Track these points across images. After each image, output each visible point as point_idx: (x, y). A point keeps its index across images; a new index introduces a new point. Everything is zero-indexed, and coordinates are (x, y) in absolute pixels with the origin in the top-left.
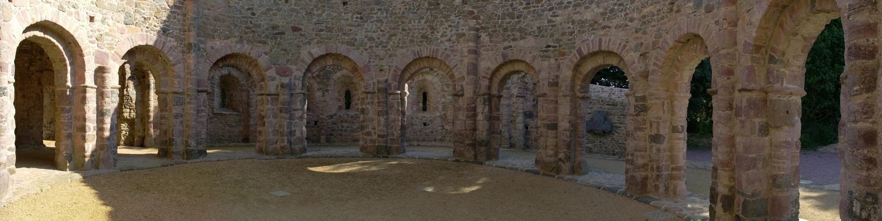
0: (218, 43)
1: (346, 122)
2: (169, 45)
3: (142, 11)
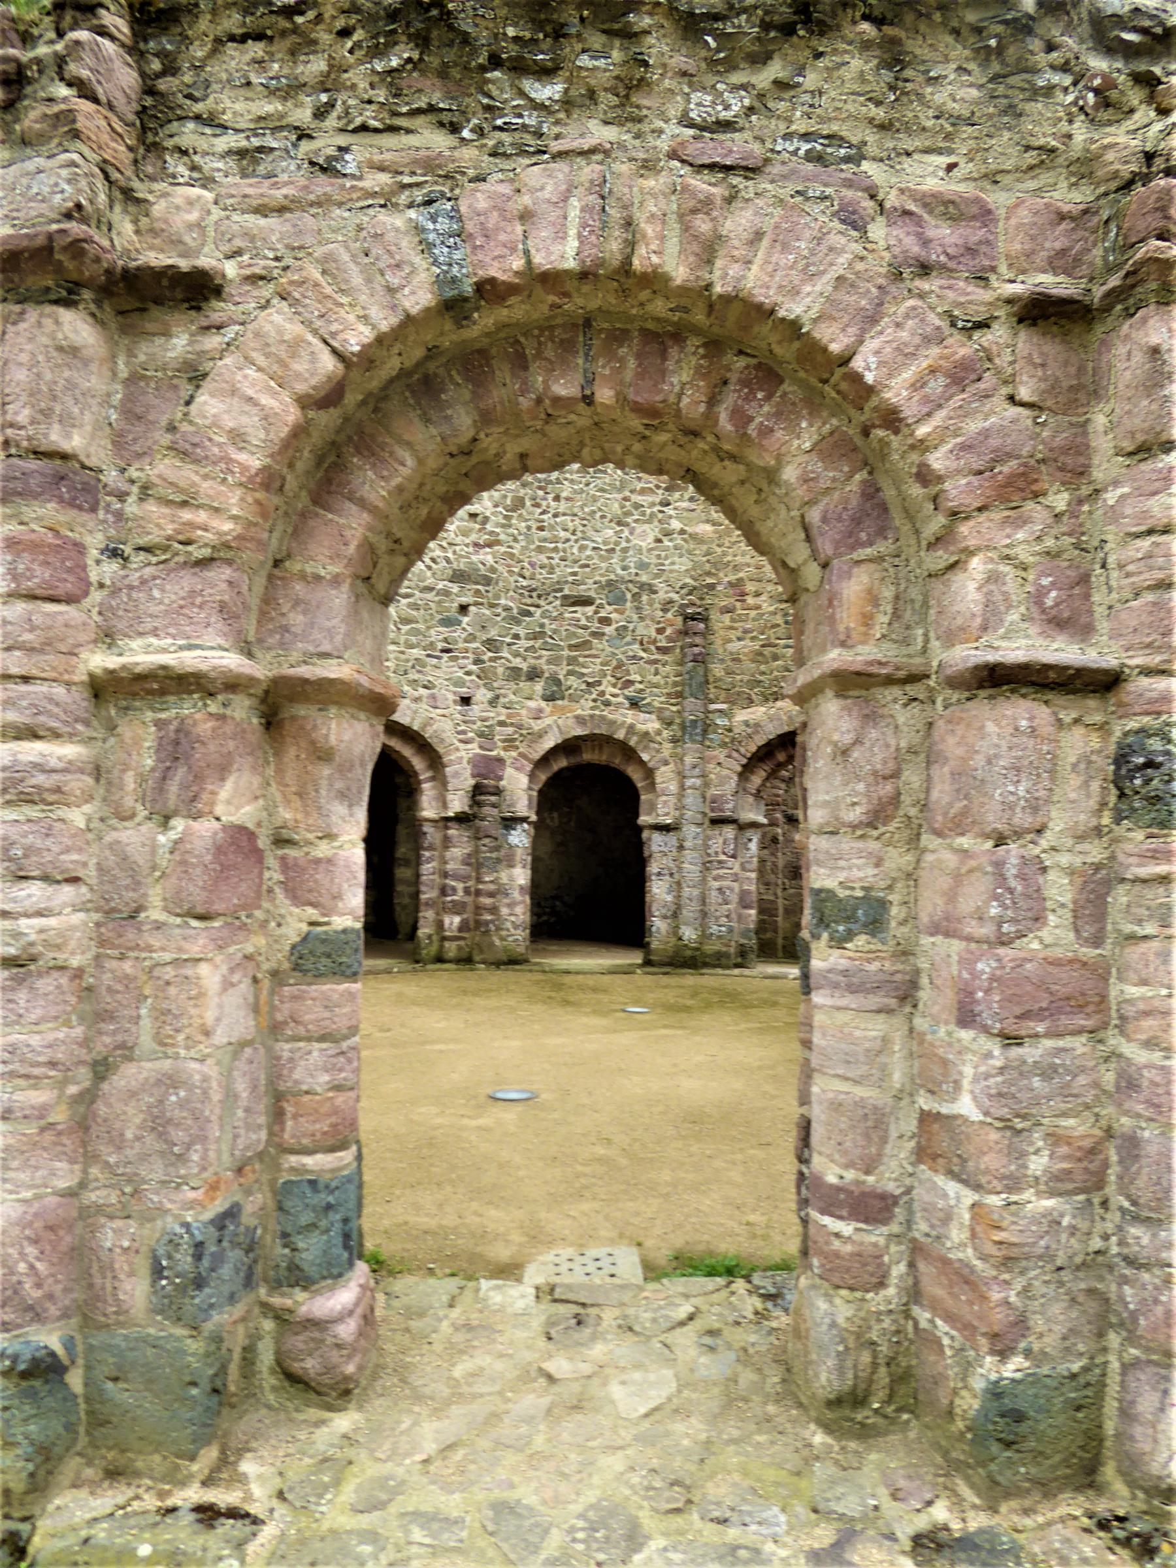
0: (758, 713)
3: (584, 671)
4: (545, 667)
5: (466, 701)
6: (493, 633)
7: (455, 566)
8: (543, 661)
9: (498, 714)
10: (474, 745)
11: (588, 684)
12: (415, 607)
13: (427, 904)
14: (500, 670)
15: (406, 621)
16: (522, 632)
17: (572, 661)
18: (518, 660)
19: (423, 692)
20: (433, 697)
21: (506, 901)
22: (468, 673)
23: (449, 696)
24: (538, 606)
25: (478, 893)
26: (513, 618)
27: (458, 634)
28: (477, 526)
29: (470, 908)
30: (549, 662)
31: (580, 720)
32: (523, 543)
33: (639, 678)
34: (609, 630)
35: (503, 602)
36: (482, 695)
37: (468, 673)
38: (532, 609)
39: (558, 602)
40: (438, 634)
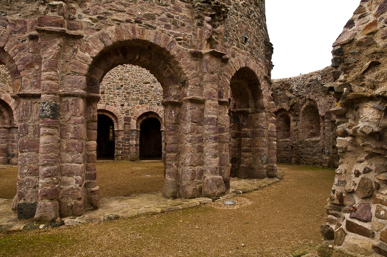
1: (309, 146)
2: (160, 110)
3: (148, 98)
4: (140, 97)
5: (122, 105)
6: (129, 91)
7: (120, 77)
8: (139, 96)
9: (130, 108)
10: (125, 114)
11: (149, 101)
12: (111, 86)
13: (116, 148)
14: (130, 99)
15: (109, 89)
16: (135, 90)
17: (145, 96)
18: (134, 96)
19: (113, 104)
20: (115, 105)
21: (132, 147)
22: (123, 99)
23: (119, 104)
24: (138, 84)
25: (125, 146)
26: (133, 87)
27: (121, 91)
28: (125, 68)
29: (123, 149)
30: (141, 96)
31: (147, 109)
32: (135, 71)
33: (159, 99)
34: (153, 89)
35: (131, 84)
36: (126, 104)
37: (123, 99)
38: (137, 85)
39: (142, 83)
40: (117, 91)
